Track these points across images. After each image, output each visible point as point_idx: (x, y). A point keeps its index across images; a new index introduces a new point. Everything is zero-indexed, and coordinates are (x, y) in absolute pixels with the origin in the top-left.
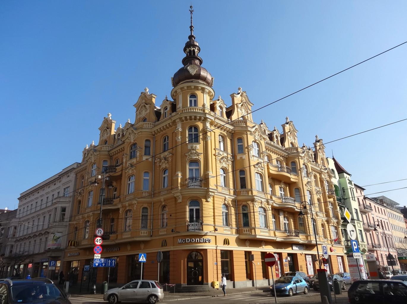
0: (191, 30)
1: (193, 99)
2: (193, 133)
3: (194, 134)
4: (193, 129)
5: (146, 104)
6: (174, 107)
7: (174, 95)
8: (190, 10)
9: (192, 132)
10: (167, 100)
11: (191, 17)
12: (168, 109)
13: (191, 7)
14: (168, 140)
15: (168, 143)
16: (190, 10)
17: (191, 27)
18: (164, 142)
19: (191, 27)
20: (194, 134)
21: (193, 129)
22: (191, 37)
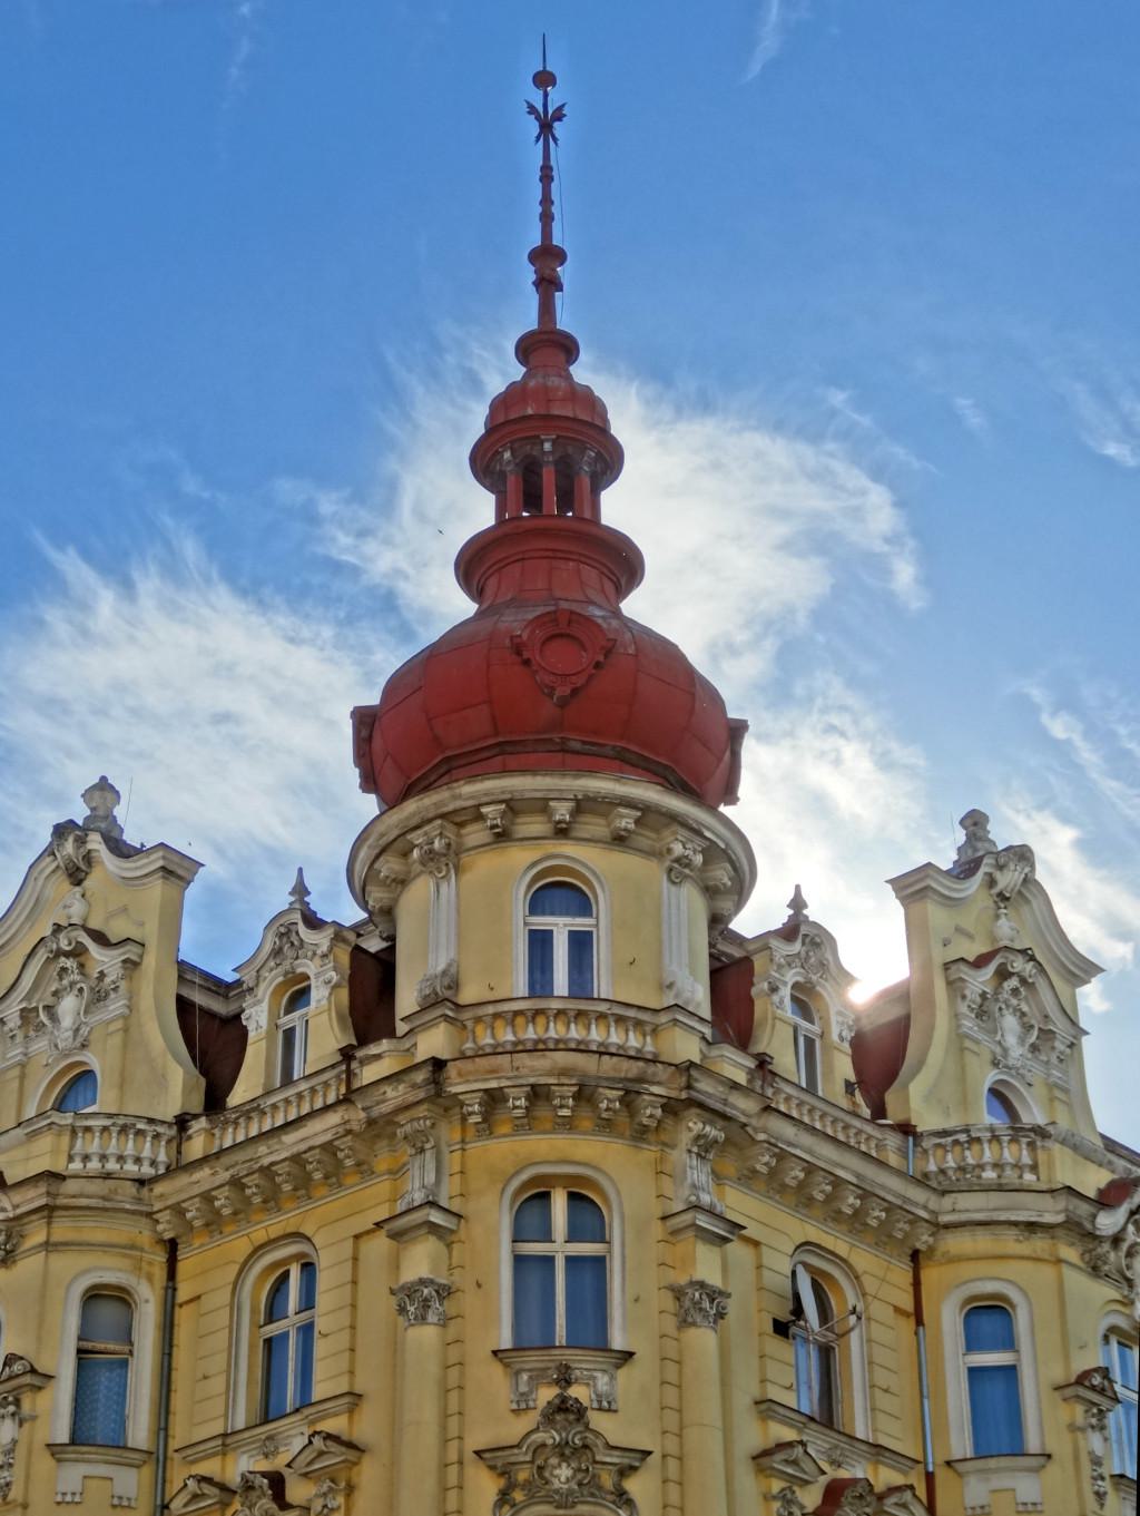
0: (548, 285)
1: (561, 927)
2: (560, 1247)
3: (570, 1260)
4: (559, 1203)
5: (100, 938)
6: (371, 985)
7: (379, 868)
8: (532, 110)
10: (313, 922)
12: (318, 994)
13: (544, 79)
14: (308, 1303)
15: (307, 1330)
16: (532, 110)
18: (270, 1319)
20: (570, 1260)
21: (559, 1203)
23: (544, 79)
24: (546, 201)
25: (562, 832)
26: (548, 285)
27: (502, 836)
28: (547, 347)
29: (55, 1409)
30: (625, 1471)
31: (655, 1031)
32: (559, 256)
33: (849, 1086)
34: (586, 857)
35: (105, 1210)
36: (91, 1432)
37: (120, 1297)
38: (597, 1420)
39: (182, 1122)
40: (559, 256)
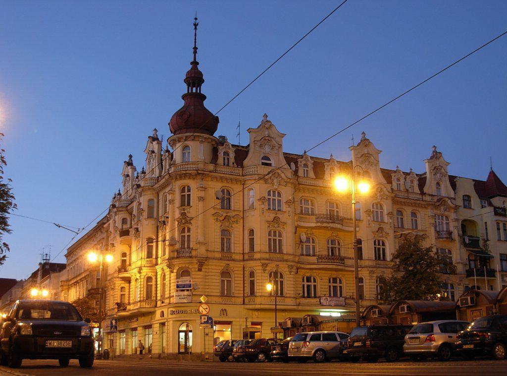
0: (195, 52)
2: (186, 193)
9: (185, 192)
11: (196, 34)
13: (196, 19)
17: (195, 48)
19: (195, 48)
22: (195, 63)
23: (196, 19)
24: (195, 39)
25: (186, 140)
26: (195, 52)
27: (179, 141)
28: (195, 63)
29: (145, 214)
30: (190, 220)
31: (198, 164)
32: (197, 48)
33: (233, 163)
34: (187, 143)
35: (149, 189)
36: (150, 216)
37: (153, 200)
38: (188, 214)
39: (158, 177)
40: (197, 48)
